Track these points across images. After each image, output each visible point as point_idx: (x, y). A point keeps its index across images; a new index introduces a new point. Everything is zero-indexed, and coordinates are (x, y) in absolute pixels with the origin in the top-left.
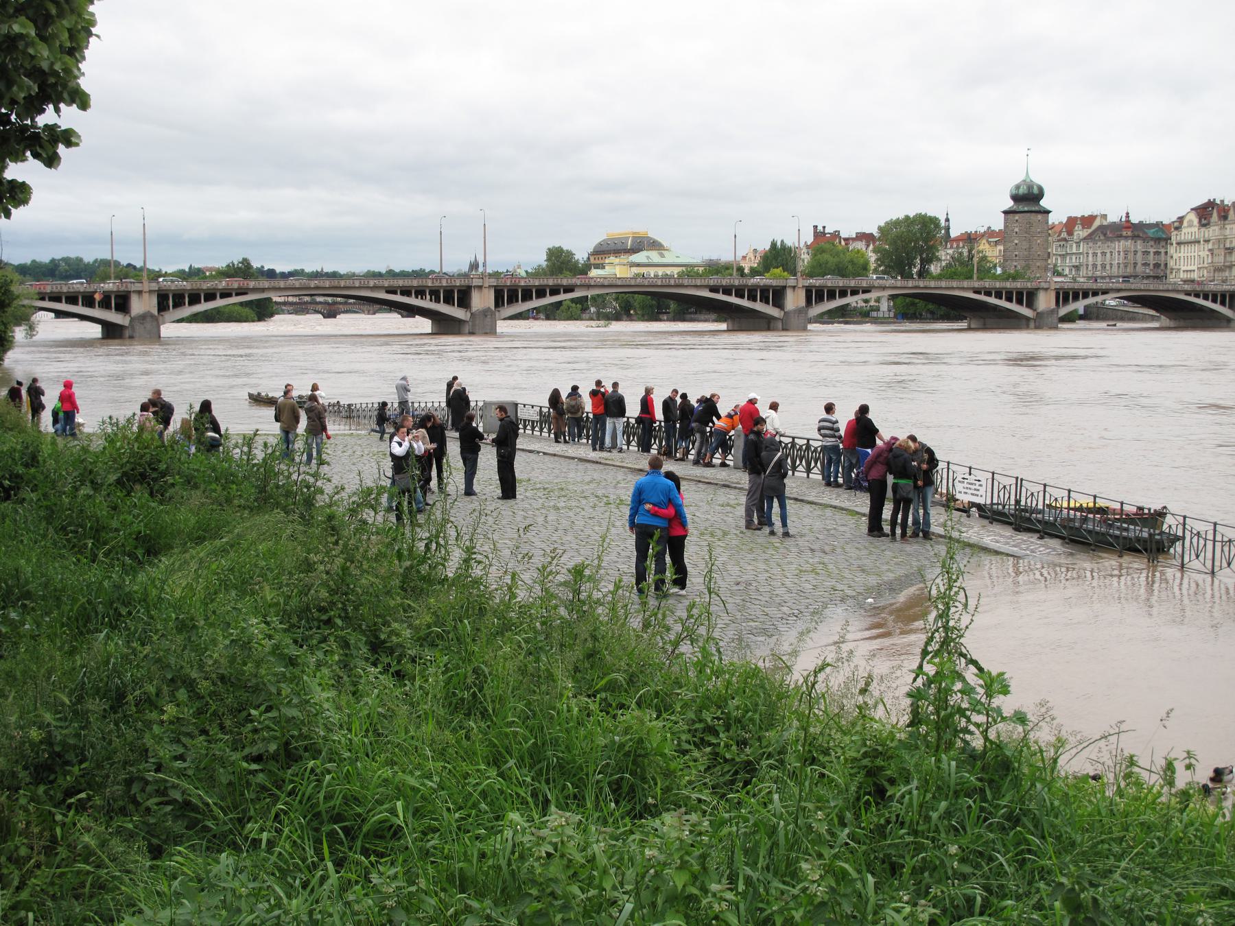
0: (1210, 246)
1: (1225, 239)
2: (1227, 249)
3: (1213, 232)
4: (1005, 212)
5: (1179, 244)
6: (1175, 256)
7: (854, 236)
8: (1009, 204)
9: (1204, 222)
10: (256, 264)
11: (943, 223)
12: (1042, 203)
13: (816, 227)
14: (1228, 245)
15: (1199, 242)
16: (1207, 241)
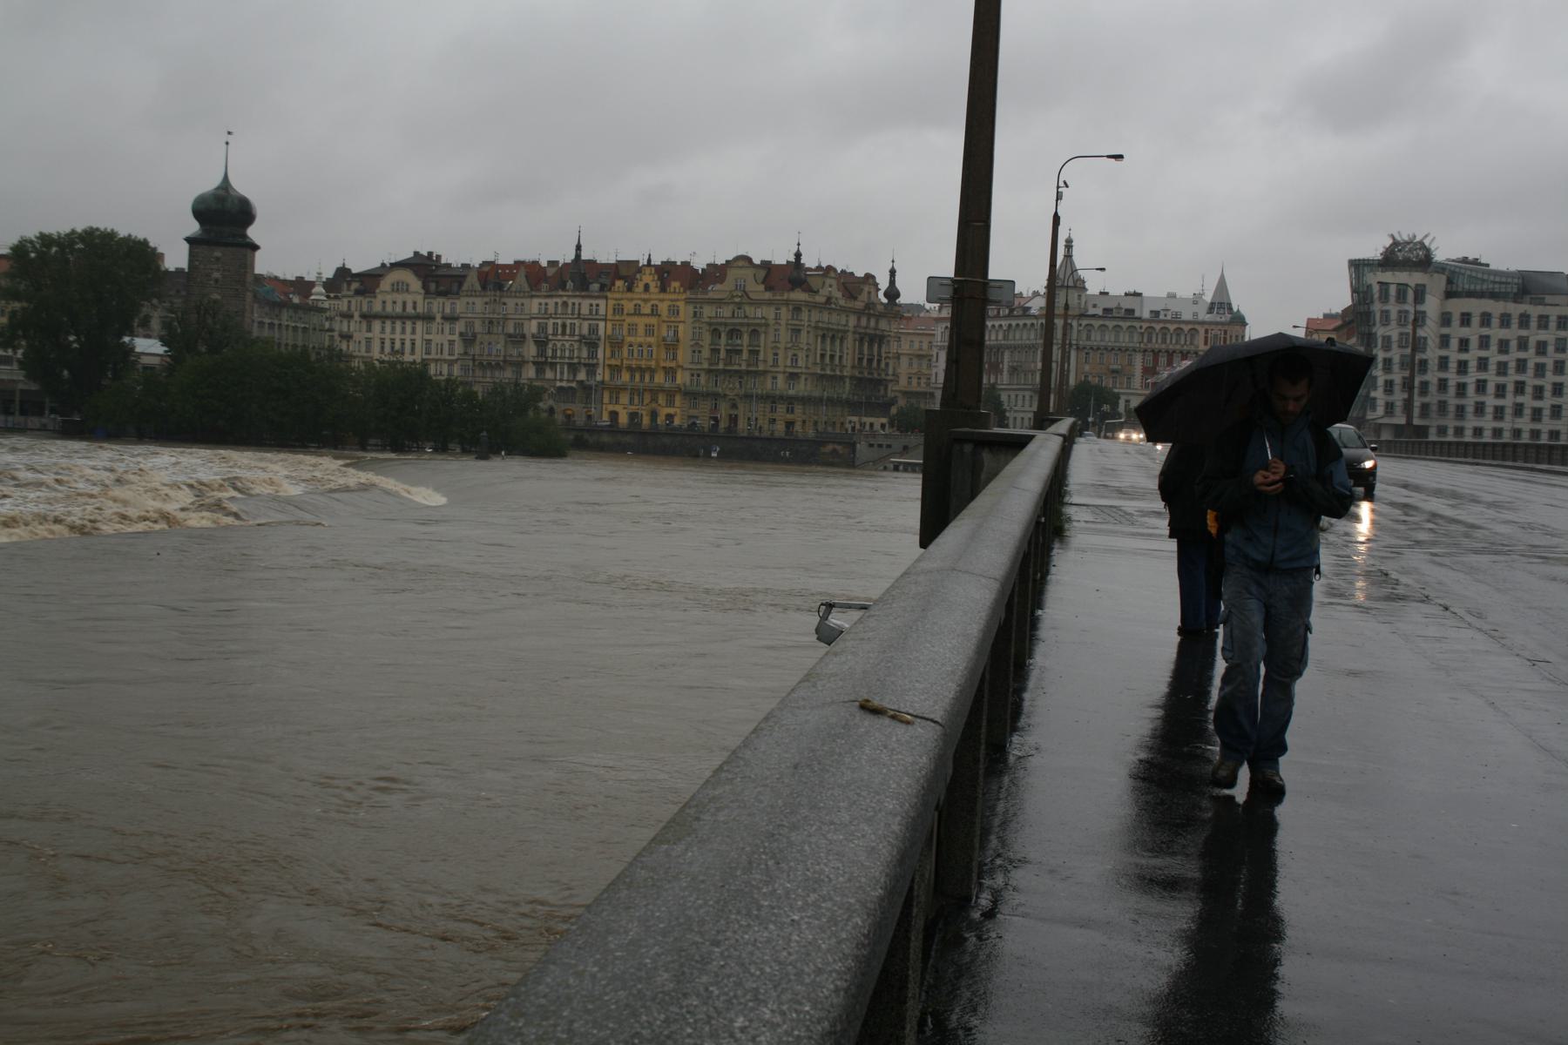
0: (460, 326)
2: (510, 336)
3: (472, 306)
4: (188, 240)
5: (368, 317)
6: (357, 336)
8: (193, 227)
9: (433, 286)
10: (356, 269)
11: (884, 284)
12: (253, 233)
14: (511, 330)
15: (428, 318)
16: (451, 319)
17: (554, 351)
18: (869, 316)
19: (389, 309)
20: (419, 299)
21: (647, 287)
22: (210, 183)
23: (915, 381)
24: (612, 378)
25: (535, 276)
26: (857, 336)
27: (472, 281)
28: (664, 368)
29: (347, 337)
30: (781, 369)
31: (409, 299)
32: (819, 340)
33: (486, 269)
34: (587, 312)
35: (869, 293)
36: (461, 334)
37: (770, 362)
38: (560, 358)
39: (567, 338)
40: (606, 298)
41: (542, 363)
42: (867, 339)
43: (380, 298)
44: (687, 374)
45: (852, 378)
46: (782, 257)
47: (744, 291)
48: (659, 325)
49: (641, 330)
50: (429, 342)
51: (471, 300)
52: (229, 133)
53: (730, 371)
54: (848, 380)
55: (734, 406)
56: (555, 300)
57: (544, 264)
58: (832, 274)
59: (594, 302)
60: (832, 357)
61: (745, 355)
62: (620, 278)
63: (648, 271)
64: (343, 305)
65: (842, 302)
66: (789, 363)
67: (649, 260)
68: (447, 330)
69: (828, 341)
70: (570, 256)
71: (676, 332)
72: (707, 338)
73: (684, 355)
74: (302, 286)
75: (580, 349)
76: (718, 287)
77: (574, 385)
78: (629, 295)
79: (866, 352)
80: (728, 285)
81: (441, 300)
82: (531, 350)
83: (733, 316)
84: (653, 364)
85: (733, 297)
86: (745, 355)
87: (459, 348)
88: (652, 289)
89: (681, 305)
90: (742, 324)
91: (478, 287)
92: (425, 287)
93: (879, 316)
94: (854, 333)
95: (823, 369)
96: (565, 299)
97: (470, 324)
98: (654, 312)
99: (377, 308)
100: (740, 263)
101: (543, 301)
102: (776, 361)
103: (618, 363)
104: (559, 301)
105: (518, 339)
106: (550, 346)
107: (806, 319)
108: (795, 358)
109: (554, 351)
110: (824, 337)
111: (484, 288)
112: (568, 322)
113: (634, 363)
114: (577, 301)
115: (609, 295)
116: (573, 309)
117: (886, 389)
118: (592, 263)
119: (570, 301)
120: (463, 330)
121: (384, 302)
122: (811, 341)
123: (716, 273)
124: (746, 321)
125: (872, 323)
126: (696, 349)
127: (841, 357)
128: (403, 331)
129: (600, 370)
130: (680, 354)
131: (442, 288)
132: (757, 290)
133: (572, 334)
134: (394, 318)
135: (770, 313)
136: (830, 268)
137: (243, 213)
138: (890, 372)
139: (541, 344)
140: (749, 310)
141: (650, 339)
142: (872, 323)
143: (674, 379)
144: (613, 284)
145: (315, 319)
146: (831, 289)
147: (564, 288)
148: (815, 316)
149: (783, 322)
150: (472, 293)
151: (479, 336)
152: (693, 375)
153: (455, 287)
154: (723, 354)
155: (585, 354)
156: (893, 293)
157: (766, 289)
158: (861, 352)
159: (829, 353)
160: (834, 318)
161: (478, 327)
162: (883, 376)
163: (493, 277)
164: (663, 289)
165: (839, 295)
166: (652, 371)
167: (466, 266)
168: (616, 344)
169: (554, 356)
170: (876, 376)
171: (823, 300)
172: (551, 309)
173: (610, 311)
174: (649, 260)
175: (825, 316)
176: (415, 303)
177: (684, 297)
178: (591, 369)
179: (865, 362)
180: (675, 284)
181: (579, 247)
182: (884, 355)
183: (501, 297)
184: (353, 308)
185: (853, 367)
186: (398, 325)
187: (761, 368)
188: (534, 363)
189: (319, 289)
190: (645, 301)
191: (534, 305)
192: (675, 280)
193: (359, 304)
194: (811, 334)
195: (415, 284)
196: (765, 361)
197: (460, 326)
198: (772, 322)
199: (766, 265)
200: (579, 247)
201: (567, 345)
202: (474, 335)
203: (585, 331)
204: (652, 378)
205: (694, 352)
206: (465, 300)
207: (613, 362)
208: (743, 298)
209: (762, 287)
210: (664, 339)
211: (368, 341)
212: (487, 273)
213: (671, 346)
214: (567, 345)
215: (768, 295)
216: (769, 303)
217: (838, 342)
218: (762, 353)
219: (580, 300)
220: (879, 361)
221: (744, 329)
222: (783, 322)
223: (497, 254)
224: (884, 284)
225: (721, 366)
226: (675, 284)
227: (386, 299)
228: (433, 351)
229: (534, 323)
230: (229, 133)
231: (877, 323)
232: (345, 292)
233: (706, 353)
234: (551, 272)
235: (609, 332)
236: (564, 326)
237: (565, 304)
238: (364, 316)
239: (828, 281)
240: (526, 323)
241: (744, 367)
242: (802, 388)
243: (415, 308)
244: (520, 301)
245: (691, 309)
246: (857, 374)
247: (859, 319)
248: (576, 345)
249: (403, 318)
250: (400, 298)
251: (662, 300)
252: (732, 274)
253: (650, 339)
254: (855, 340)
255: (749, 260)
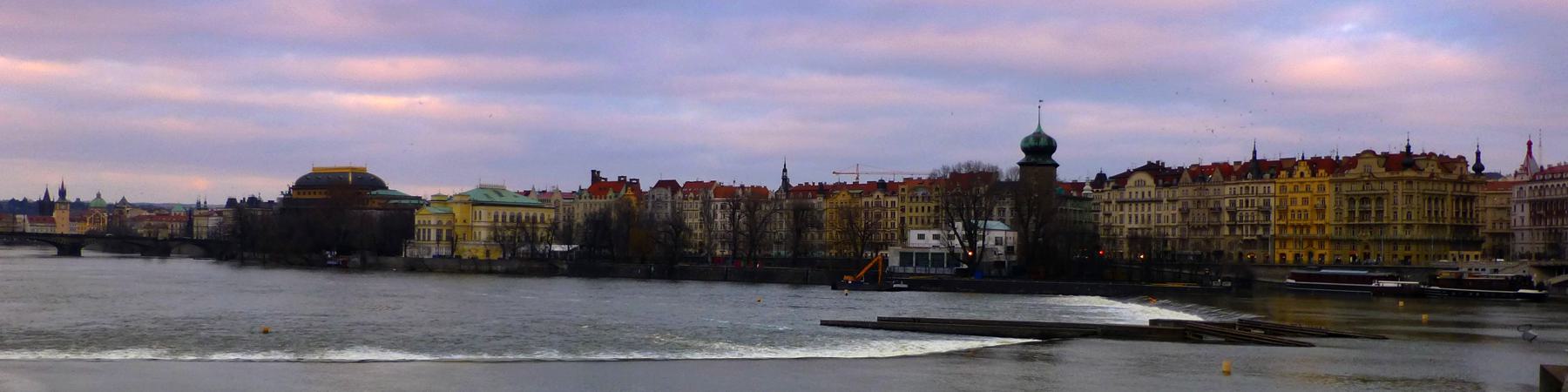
1: (1208, 199)
3: (1182, 192)
5: (1121, 203)
6: (1114, 214)
7: (617, 180)
8: (1023, 156)
9: (1161, 182)
12: (1055, 157)
13: (593, 171)
14: (1211, 205)
15: (1159, 201)
16: (1174, 201)
17: (1241, 217)
18: (1462, 184)
19: (1134, 197)
20: (1153, 190)
21: (1302, 174)
22: (1032, 130)
23: (1498, 226)
24: (1281, 231)
25: (1226, 171)
26: (1454, 198)
27: (1186, 177)
28: (1317, 224)
29: (1109, 215)
30: (1399, 222)
31: (1146, 190)
32: (1426, 201)
33: (1194, 169)
34: (1262, 192)
35: (1461, 168)
36: (1180, 210)
37: (1392, 218)
38: (1246, 221)
39: (1249, 209)
40: (1275, 183)
41: (1232, 225)
42: (1461, 198)
43: (1127, 191)
44: (1333, 229)
45: (1451, 226)
46: (1396, 148)
47: (1371, 173)
48: (1312, 198)
49: (1300, 202)
50: (1159, 215)
51: (1185, 188)
52: (1040, 101)
53: (1362, 225)
54: (1448, 228)
55: (1367, 247)
56: (1241, 186)
57: (1232, 164)
58: (1433, 158)
59: (1267, 186)
60: (1436, 212)
61: (1373, 214)
62: (1283, 170)
63: (1302, 163)
64: (1105, 196)
65: (1442, 176)
66: (1405, 218)
67: (1303, 157)
68: (1170, 208)
69: (1433, 202)
70: (1249, 158)
71: (1324, 201)
72: (1346, 205)
73: (1330, 216)
74: (1078, 186)
75: (1258, 215)
76: (1352, 171)
77: (1255, 238)
78: (1291, 180)
79: (1461, 207)
80: (1359, 169)
81: (1166, 190)
82: (1226, 217)
83: (1364, 189)
84: (1308, 222)
85: (1363, 177)
86: (1373, 214)
87: (1178, 218)
88: (1305, 176)
89: (1327, 184)
90: (1371, 194)
91: (1190, 180)
92: (1156, 182)
93: (1470, 183)
94: (1452, 195)
95: (1430, 220)
96: (1247, 185)
97: (1185, 203)
98: (1308, 190)
99: (1126, 196)
100: (1367, 155)
101: (1233, 187)
102: (1395, 218)
103: (1284, 223)
104: (1244, 186)
105: (1217, 211)
106: (1238, 214)
107: (1416, 188)
108: (1409, 216)
109: (1241, 217)
110: (1430, 200)
111: (1194, 181)
112: (1250, 199)
113: (1295, 223)
114: (1255, 186)
115: (1276, 180)
116: (1253, 191)
117: (1477, 231)
118: (1264, 161)
119: (1250, 186)
120: (1181, 207)
121: (1130, 193)
122: (1421, 202)
123: (1352, 162)
124: (1373, 192)
125: (1465, 188)
126: (1338, 212)
127: (1443, 212)
128: (1143, 210)
129: (1272, 228)
130: (1327, 214)
131: (1166, 182)
132: (1380, 172)
133: (1253, 206)
134: (1137, 202)
135: (1389, 186)
136: (1432, 154)
137: (1051, 146)
138: (1480, 220)
139: (1232, 214)
140: (1376, 185)
141: (1306, 207)
142: (1465, 188)
143: (1324, 231)
144: (1279, 173)
145: (1086, 205)
146: (1430, 168)
147: (1246, 178)
148: (1423, 186)
149: (1400, 192)
150: (1187, 185)
151: (1191, 211)
152: (1336, 228)
153: (1175, 181)
154: (1357, 215)
155: (1262, 218)
156: (1479, 167)
157: (1387, 170)
158: (1457, 208)
159: (1433, 210)
160: (1436, 187)
161: (1190, 205)
162: (1475, 223)
163: (1199, 174)
164: (1314, 175)
165: (1439, 171)
166: (1308, 227)
167: (1181, 169)
168: (1283, 213)
169: (1241, 221)
170: (1469, 223)
171: (1428, 175)
172: (1238, 192)
173: (1278, 191)
174: (1303, 157)
175: (1430, 186)
176: (1150, 192)
177: (1328, 179)
178: (1266, 228)
179: (1461, 215)
180: (1322, 171)
181: (1255, 152)
182: (1474, 209)
183: (1205, 185)
184: (1111, 197)
185: (1452, 218)
186: (1140, 206)
187: (1385, 222)
188: (1228, 225)
189: (1087, 187)
190: (1302, 183)
191: (1227, 190)
192: (1321, 168)
193: (1115, 195)
194: (1421, 198)
195: (1149, 181)
196: (1388, 217)
197: (1179, 205)
198: (1391, 192)
199: (1386, 156)
200: (1255, 152)
201: (1250, 213)
202: (1188, 210)
203: (1261, 204)
204: (1308, 231)
205: (1337, 213)
206: (1181, 189)
207: (1281, 222)
208: (1369, 179)
209: (1384, 169)
210: (1315, 206)
211: (1122, 216)
212: (1194, 172)
213: (1321, 211)
214: (1250, 213)
215: (1388, 175)
216: (1389, 179)
217: (1440, 202)
218: (1385, 212)
219: (1258, 185)
220: (1471, 213)
221: (1372, 197)
222: (1400, 192)
223: (1390, 146)
224: (1472, 161)
225: (1356, 222)
226: (1322, 171)
227: (1131, 190)
228: (1162, 219)
229: (1227, 201)
230: (1040, 101)
231: (1468, 187)
232: (1106, 188)
233: (1346, 214)
234: (1236, 168)
235: (1278, 203)
236: (1247, 201)
237: (1247, 188)
238: (1118, 202)
239: (1431, 163)
240: (1222, 201)
241: (1373, 222)
242: (1416, 233)
243: (1150, 195)
244: (1217, 188)
245: (1334, 187)
246: (1455, 223)
247: (1455, 187)
248: (1256, 213)
249: (1143, 202)
250: (1140, 190)
251: (1313, 182)
252: (1360, 162)
253: (1306, 207)
254: (1452, 200)
255: (1373, 153)
